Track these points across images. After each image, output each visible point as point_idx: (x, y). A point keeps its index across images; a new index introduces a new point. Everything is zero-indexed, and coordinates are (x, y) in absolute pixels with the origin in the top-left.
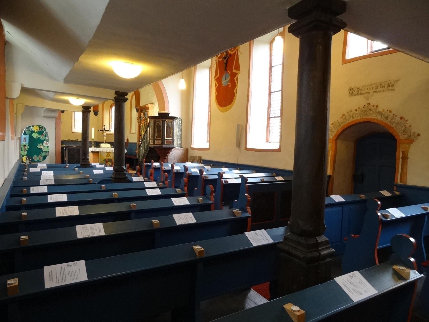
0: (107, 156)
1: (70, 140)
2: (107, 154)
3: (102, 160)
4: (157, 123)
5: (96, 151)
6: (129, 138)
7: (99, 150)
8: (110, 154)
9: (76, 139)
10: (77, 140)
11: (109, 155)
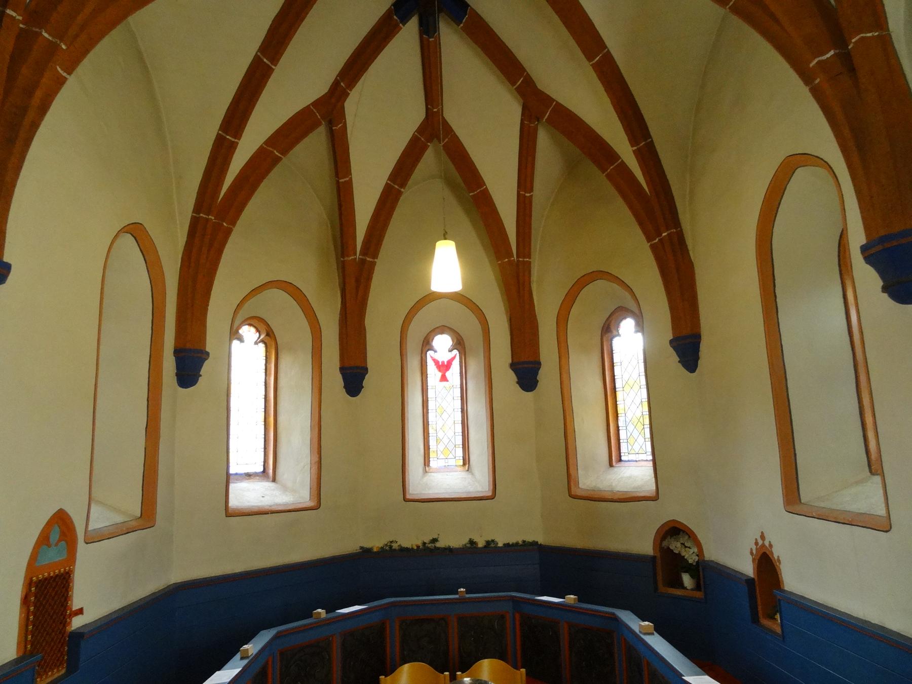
1: (395, 546)
6: (778, 552)
9: (427, 541)
10: (434, 541)
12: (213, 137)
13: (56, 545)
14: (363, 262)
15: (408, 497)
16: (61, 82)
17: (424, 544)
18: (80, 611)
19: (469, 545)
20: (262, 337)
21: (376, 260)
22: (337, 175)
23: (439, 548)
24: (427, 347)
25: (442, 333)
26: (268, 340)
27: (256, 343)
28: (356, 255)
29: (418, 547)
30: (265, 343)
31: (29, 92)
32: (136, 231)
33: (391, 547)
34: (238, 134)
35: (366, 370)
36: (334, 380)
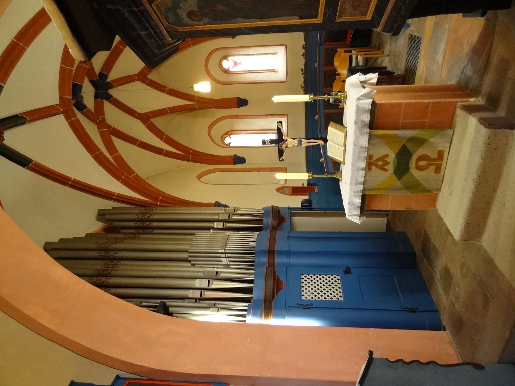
0: (383, 168)
1: (303, 85)
2: (373, 168)
3: (397, 183)
4: (186, 20)
5: (360, 205)
7: (355, 196)
8: (374, 158)
9: (302, 73)
10: (302, 70)
11: (379, 159)
12: (164, 157)
13: (284, 190)
14: (197, 101)
15: (285, 81)
17: (303, 74)
18: (303, 184)
19: (304, 56)
20: (228, 136)
21: (196, 96)
22: (167, 114)
23: (304, 69)
24: (228, 71)
25: (222, 64)
26: (229, 134)
27: (230, 138)
28: (195, 104)
29: (304, 77)
30: (230, 135)
31: (175, 200)
32: (199, 177)
33: (303, 87)
34: (163, 150)
35: (238, 98)
36: (242, 110)
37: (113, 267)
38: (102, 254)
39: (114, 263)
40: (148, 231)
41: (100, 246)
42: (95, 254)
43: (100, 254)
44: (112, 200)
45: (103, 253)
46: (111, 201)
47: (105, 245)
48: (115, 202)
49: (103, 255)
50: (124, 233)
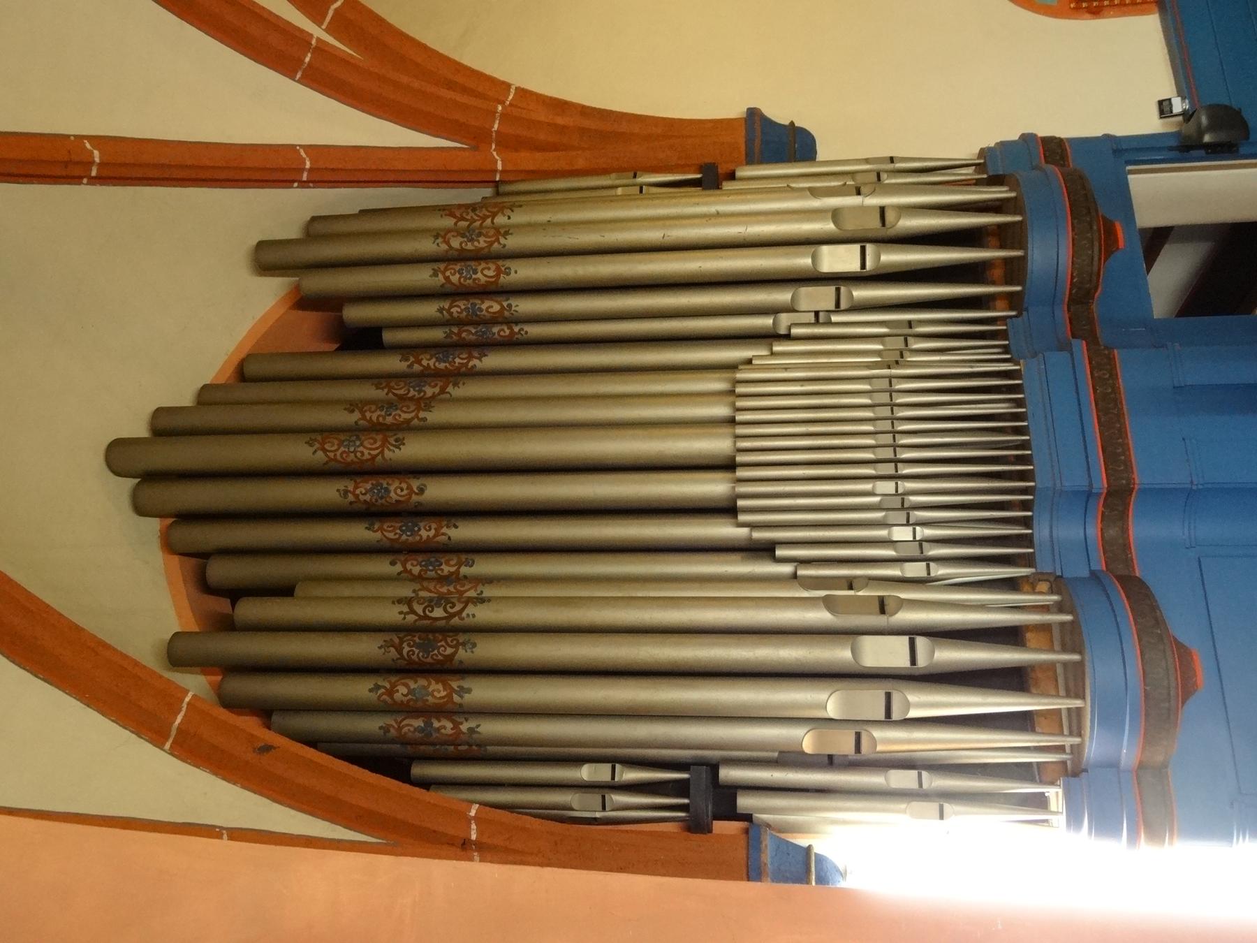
16: (523, 93)
37: (452, 616)
38: (362, 498)
39: (425, 537)
40: (502, 333)
41: (339, 457)
42: (326, 493)
43: (351, 498)
44: (296, 185)
45: (363, 491)
46: (292, 187)
47: (359, 455)
48: (310, 187)
49: (365, 500)
50: (404, 349)
